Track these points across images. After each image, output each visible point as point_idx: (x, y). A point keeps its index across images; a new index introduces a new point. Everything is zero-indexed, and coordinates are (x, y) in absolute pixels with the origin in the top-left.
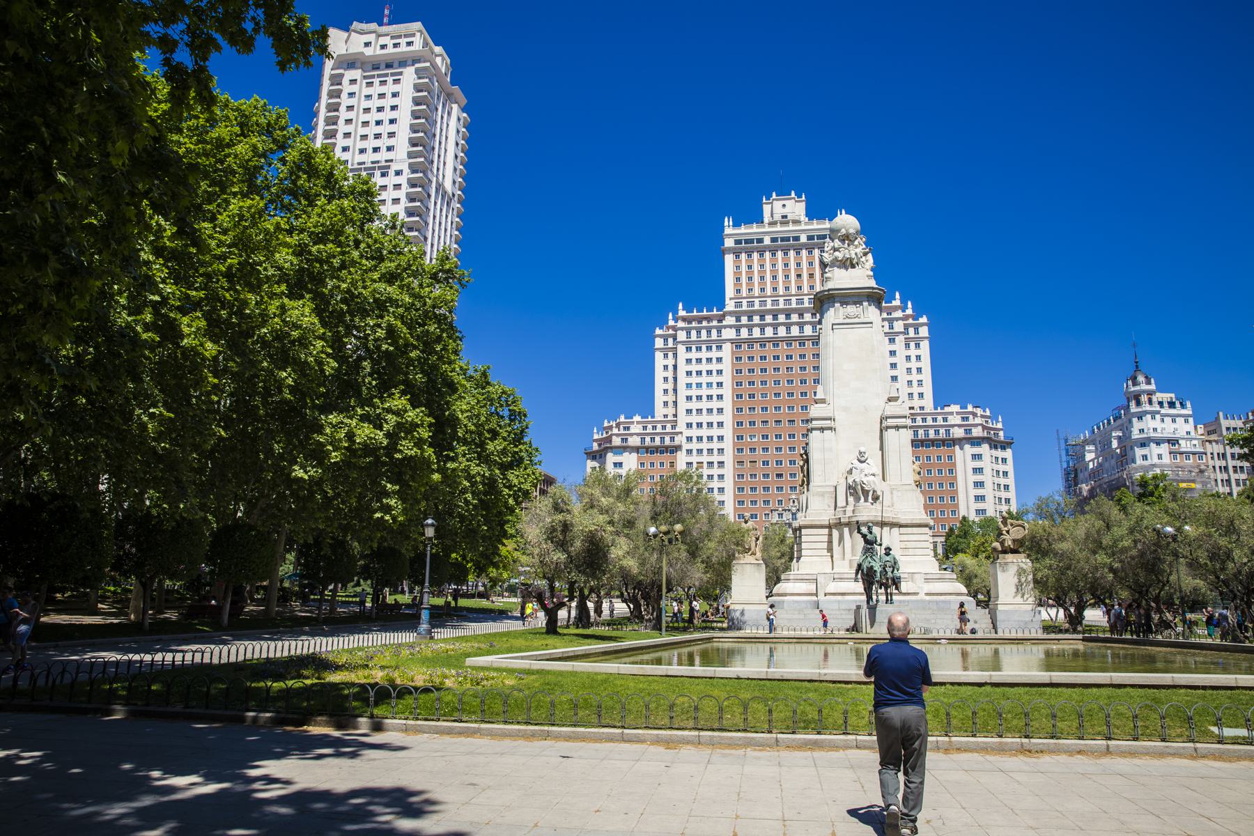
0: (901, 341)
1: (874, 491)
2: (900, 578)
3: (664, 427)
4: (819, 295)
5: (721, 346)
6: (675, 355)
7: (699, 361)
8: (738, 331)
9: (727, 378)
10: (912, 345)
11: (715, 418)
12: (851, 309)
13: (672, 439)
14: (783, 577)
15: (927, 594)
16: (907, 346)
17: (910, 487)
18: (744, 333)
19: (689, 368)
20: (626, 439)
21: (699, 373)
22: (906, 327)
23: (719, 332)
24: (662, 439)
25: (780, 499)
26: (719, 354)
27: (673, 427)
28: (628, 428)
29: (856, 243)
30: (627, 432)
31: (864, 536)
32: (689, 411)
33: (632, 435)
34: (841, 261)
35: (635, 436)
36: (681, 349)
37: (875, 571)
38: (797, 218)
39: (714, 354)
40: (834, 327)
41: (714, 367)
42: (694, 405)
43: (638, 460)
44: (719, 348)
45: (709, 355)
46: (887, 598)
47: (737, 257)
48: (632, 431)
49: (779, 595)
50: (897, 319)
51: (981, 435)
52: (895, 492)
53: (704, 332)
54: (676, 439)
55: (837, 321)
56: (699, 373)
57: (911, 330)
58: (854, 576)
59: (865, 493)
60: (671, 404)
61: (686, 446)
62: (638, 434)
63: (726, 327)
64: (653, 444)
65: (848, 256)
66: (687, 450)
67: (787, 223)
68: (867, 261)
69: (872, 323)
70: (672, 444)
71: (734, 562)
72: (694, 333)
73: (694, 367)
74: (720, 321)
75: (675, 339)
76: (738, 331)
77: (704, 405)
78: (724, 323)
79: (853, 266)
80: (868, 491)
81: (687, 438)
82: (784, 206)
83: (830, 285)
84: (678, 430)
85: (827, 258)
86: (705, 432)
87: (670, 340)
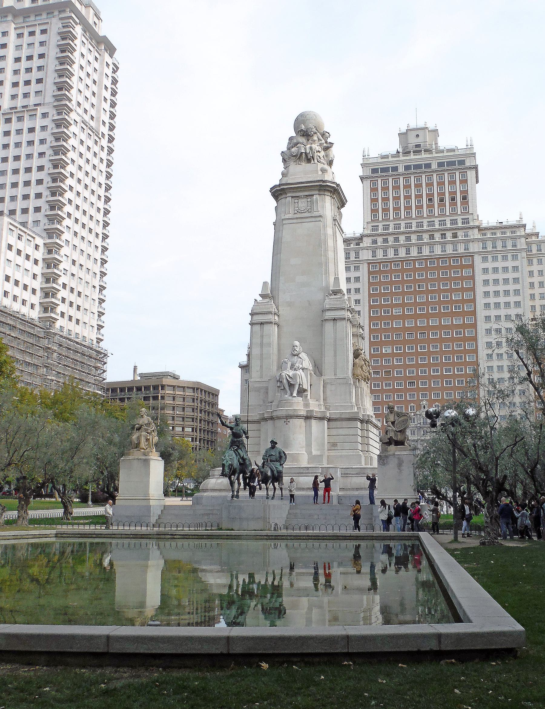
1: (299, 385)
10: (535, 261)
12: (302, 204)
16: (530, 263)
17: (341, 381)
18: (380, 254)
22: (528, 244)
25: (412, 404)
26: (357, 274)
29: (315, 138)
31: (231, 429)
38: (428, 147)
40: (284, 222)
44: (357, 268)
47: (375, 184)
52: (329, 386)
59: (291, 386)
63: (363, 248)
67: (421, 151)
69: (320, 216)
74: (358, 244)
78: (361, 245)
79: (309, 160)
82: (418, 136)
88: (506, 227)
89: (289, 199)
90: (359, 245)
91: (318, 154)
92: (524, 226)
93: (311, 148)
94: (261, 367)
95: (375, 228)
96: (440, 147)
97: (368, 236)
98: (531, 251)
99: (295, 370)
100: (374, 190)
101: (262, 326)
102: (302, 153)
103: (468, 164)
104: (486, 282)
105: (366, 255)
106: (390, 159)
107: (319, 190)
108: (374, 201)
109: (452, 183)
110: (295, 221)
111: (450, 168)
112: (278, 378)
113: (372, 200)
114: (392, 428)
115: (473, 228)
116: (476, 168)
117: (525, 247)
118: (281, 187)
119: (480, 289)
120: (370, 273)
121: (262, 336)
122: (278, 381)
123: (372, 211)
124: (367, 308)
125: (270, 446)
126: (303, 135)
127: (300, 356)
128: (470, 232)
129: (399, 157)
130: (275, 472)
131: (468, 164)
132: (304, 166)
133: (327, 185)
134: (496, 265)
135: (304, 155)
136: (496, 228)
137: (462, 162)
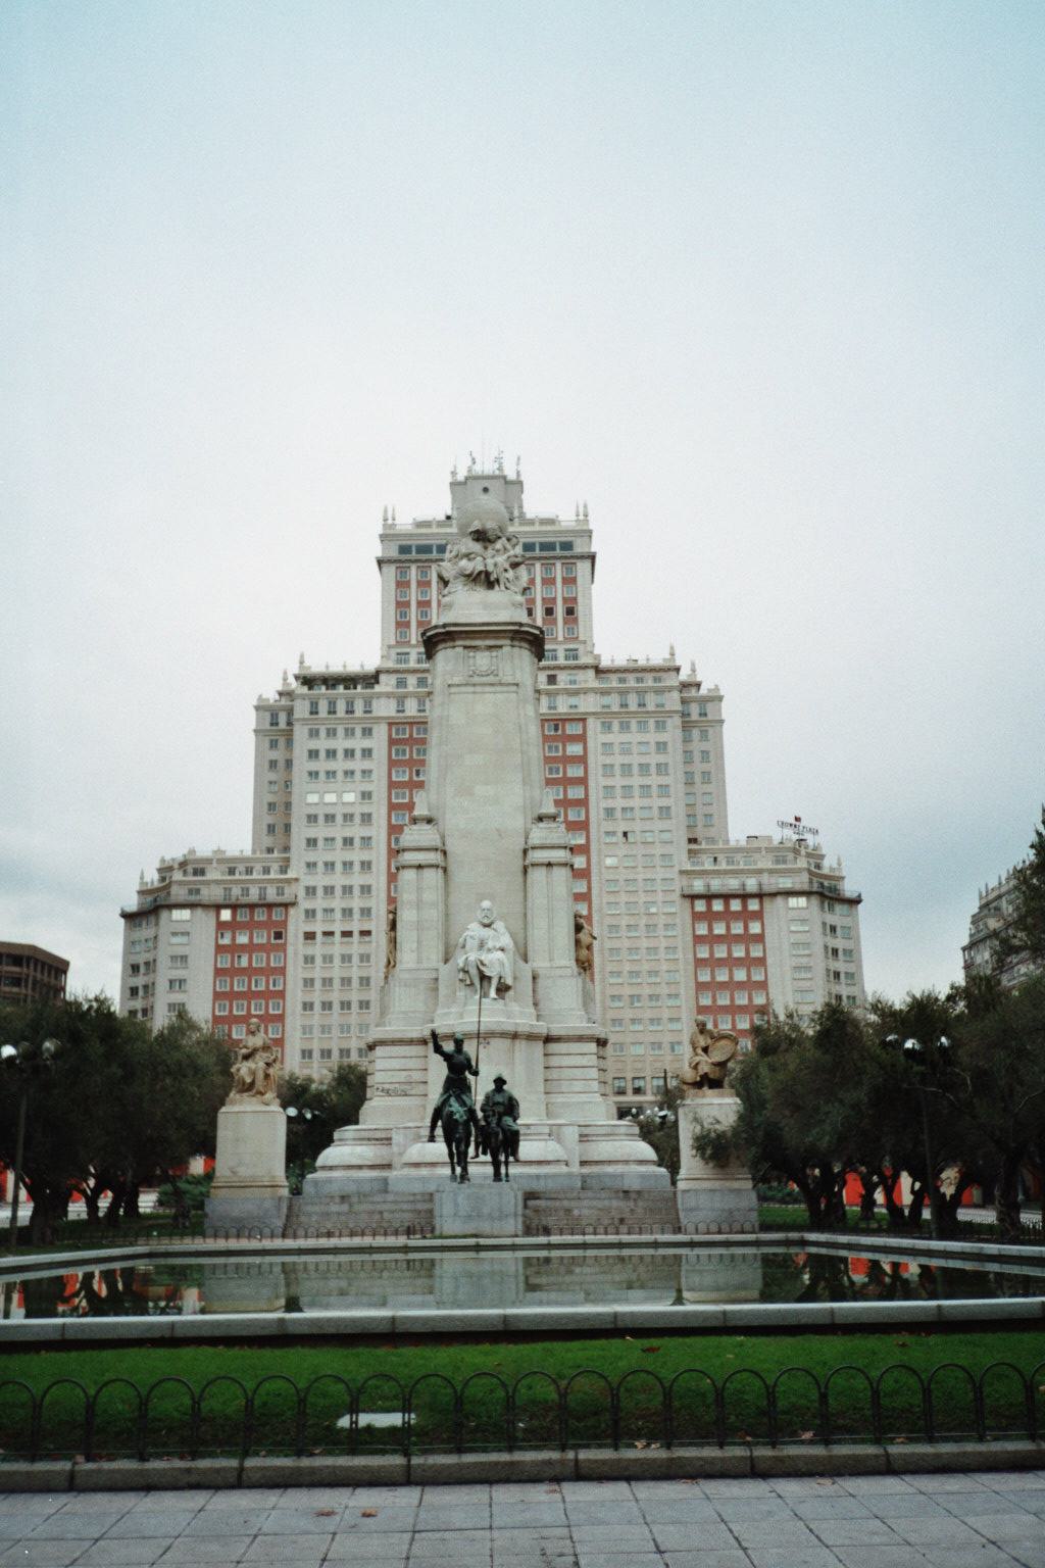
0: (675, 727)
1: (500, 978)
2: (517, 1133)
3: (266, 871)
4: (429, 634)
5: (370, 730)
6: (289, 742)
7: (331, 754)
8: (401, 700)
9: (378, 785)
10: (696, 733)
11: (356, 855)
12: (482, 660)
13: (280, 892)
14: (336, 1135)
15: (583, 1163)
19: (313, 766)
20: (198, 891)
21: (331, 774)
22: (684, 701)
23: (368, 703)
24: (263, 890)
26: (367, 743)
27: (284, 870)
28: (202, 872)
30: (200, 878)
31: (447, 1057)
32: (312, 843)
33: (208, 883)
34: (469, 576)
35: (212, 886)
36: (300, 732)
37: (456, 1120)
39: (358, 743)
40: (453, 690)
41: (357, 764)
42: (320, 831)
43: (221, 926)
44: (367, 732)
45: (349, 744)
46: (465, 1169)
48: (209, 876)
49: (323, 1168)
50: (670, 689)
51: (806, 887)
52: (540, 982)
53: (341, 707)
54: (286, 891)
55: (456, 680)
56: (331, 774)
57: (694, 709)
58: (426, 1132)
59: (484, 978)
60: (279, 829)
61: (305, 904)
62: (217, 882)
63: (379, 695)
64: (244, 900)
65: (482, 568)
66: (307, 911)
68: (517, 578)
70: (280, 899)
71: (223, 1109)
72: (323, 707)
73: (322, 765)
75: (290, 711)
76: (401, 700)
77: (339, 831)
78: (377, 688)
80: (490, 978)
81: (307, 889)
82: (486, 490)
83: (449, 617)
84: (291, 874)
85: (448, 569)
86: (338, 879)
87: (282, 718)
88: (644, 670)
89: (461, 649)
90: (373, 688)
91: (507, 575)
92: (678, 670)
93: (495, 565)
94: (419, 942)
95: (403, 657)
96: (562, 524)
97: (388, 671)
98: (689, 715)
99: (489, 950)
100: (402, 584)
101: (420, 870)
102: (480, 573)
103: (578, 549)
104: (608, 769)
105: (385, 708)
106: (435, 530)
107: (512, 639)
108: (402, 606)
109: (549, 582)
110: (471, 689)
111: (545, 554)
112: (461, 965)
113: (399, 604)
114: (703, 1058)
115: (585, 667)
116: (592, 558)
117: (678, 707)
118: (448, 629)
119: (596, 781)
120: (392, 742)
121: (419, 889)
122: (459, 971)
123: (399, 625)
124: (384, 810)
125: (492, 1086)
126: (477, 540)
127: (494, 926)
128: (581, 676)
129: (451, 526)
130: (509, 1134)
131: (578, 549)
132: (480, 594)
133: (527, 633)
134: (625, 737)
135: (483, 576)
136: (626, 670)
137: (567, 546)
